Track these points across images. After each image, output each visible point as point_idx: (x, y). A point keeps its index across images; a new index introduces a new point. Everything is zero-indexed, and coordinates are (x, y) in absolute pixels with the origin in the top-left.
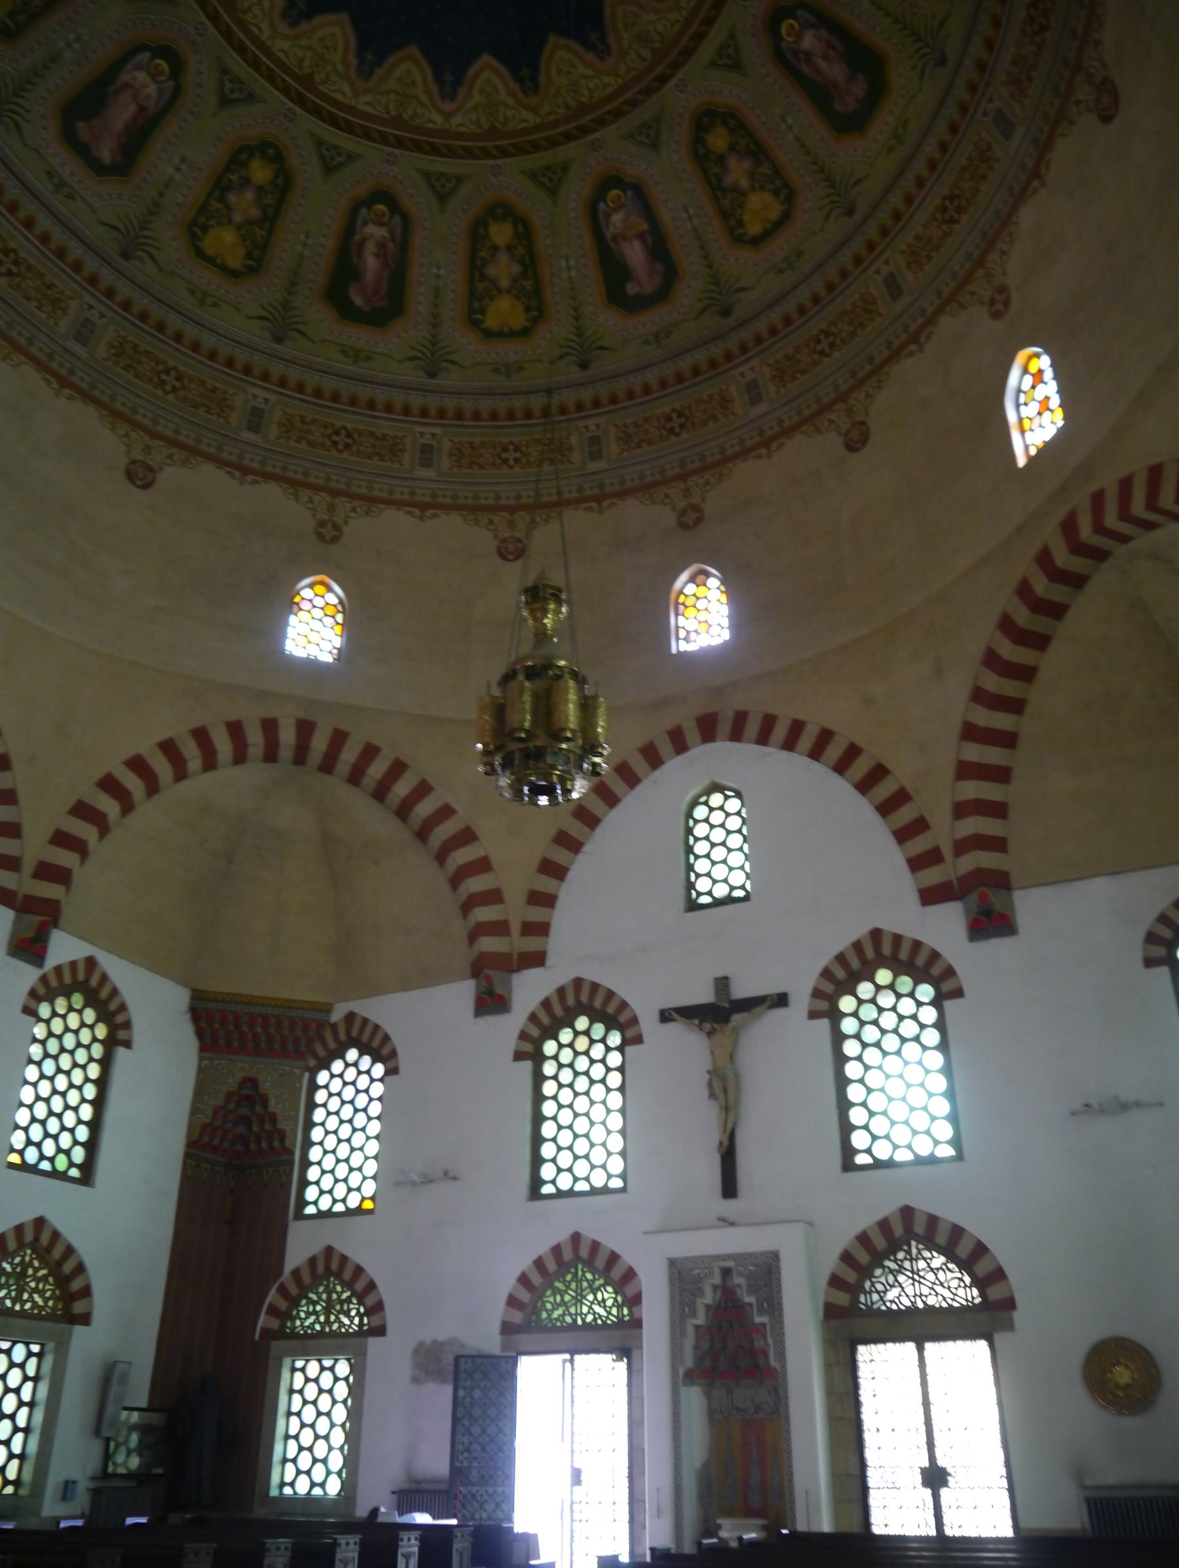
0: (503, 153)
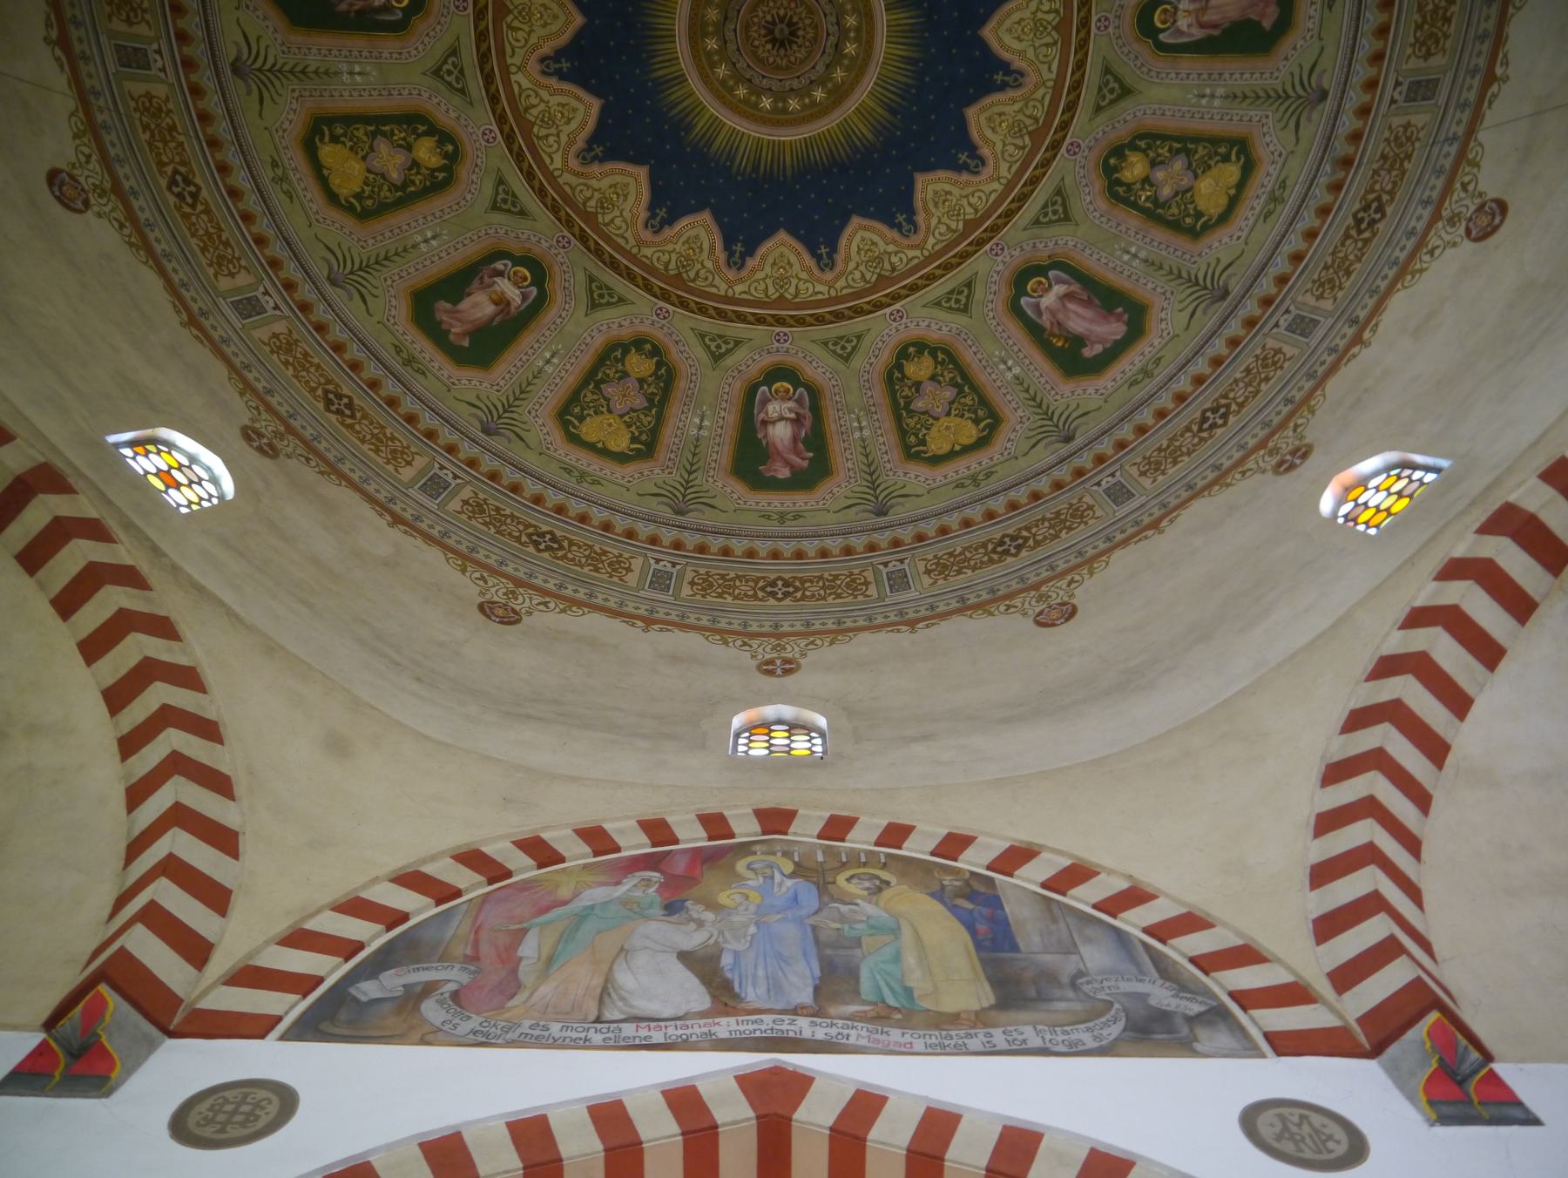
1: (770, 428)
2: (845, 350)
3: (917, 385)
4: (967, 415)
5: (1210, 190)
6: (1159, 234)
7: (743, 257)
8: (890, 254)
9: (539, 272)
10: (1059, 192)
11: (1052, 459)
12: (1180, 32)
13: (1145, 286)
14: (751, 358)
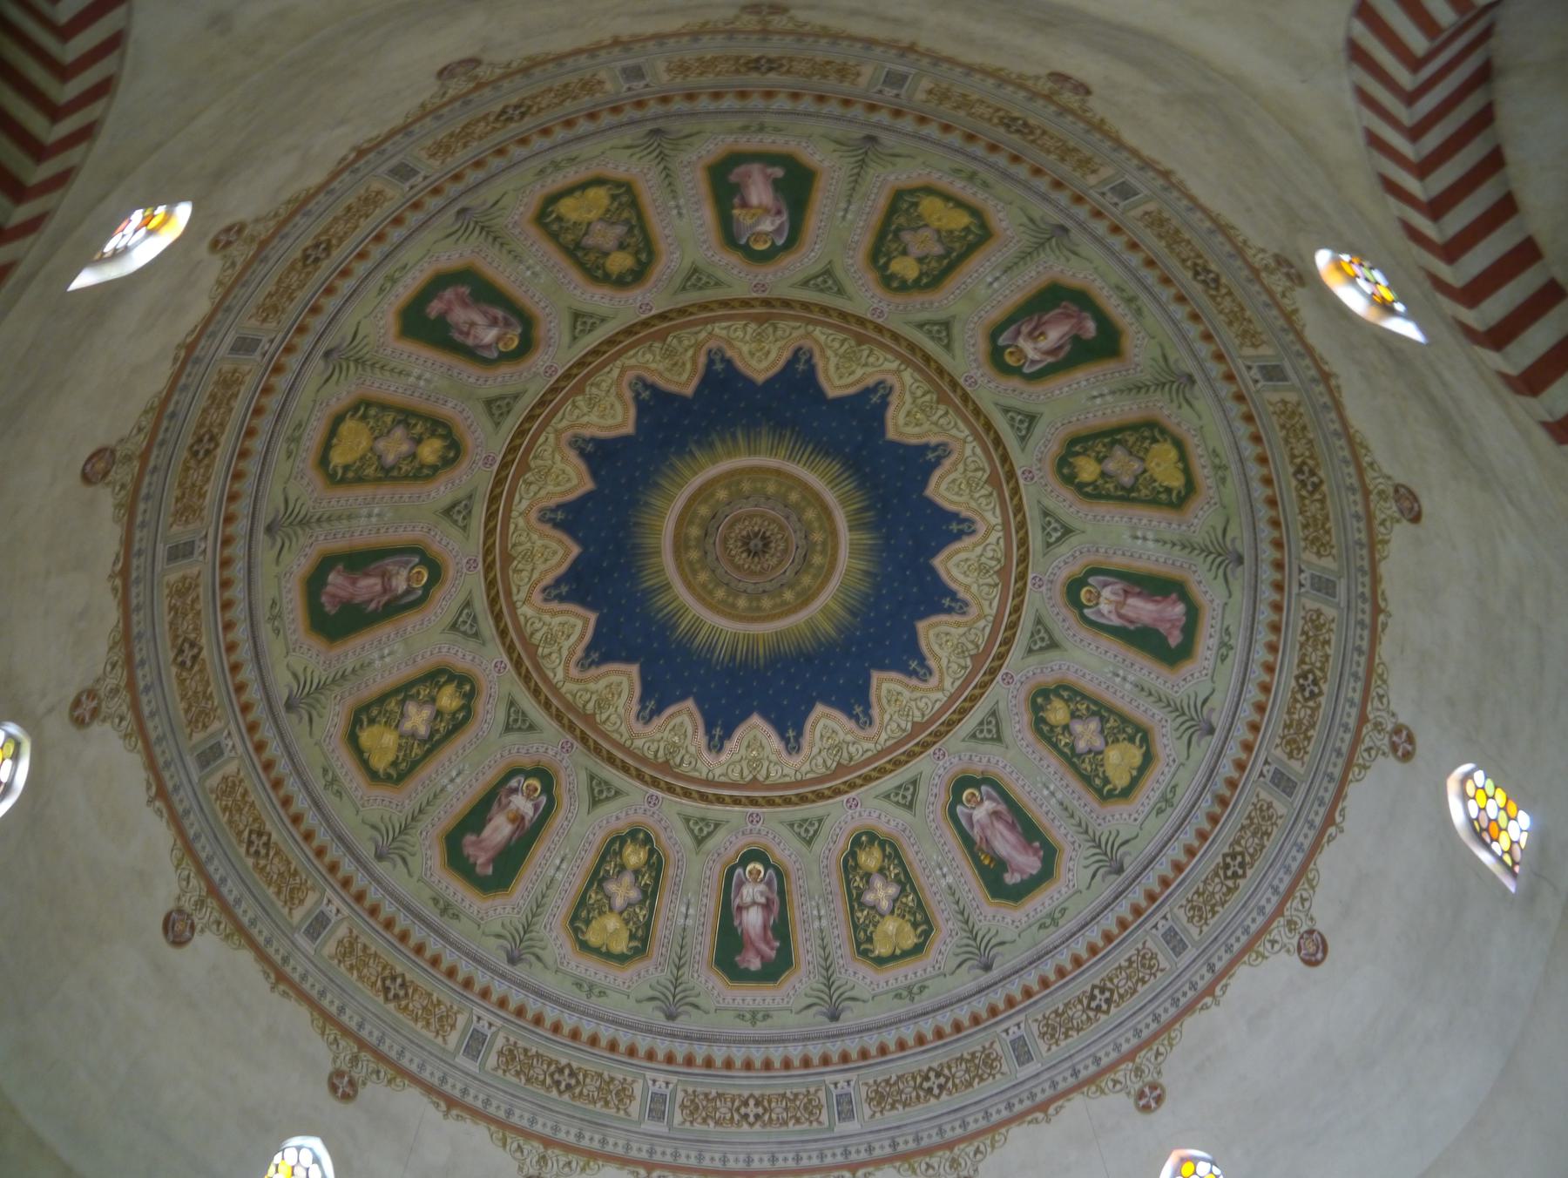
0: (861, 321)
1: (744, 913)
2: (808, 833)
3: (867, 877)
4: (907, 917)
5: (1119, 760)
6: (1076, 784)
7: (722, 740)
8: (848, 743)
9: (545, 776)
10: (994, 713)
11: (971, 986)
12: (1100, 613)
13: (1060, 832)
14: (727, 844)
